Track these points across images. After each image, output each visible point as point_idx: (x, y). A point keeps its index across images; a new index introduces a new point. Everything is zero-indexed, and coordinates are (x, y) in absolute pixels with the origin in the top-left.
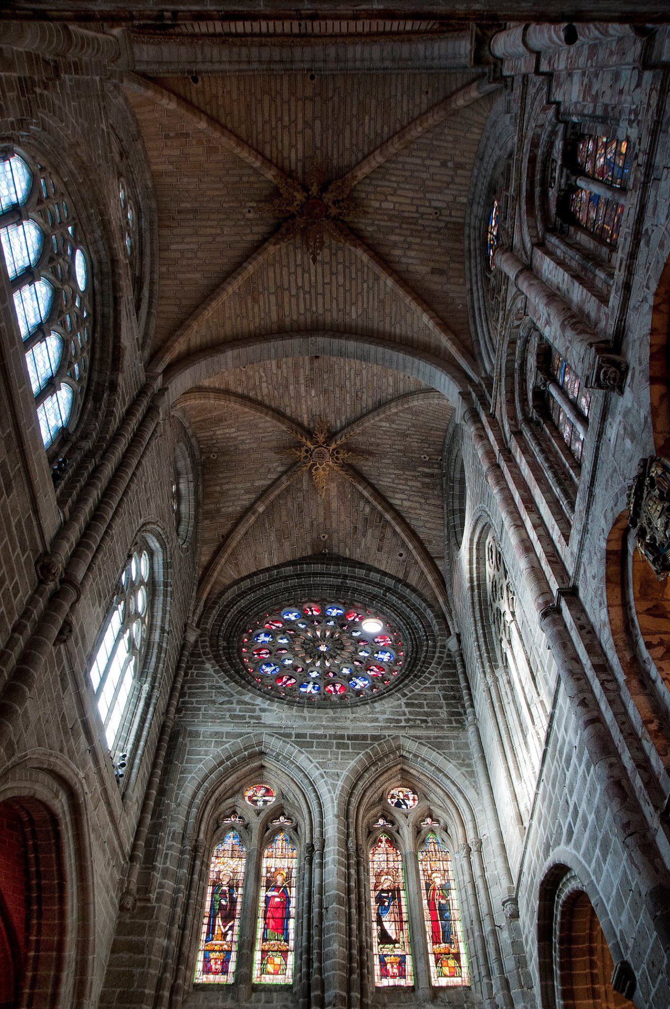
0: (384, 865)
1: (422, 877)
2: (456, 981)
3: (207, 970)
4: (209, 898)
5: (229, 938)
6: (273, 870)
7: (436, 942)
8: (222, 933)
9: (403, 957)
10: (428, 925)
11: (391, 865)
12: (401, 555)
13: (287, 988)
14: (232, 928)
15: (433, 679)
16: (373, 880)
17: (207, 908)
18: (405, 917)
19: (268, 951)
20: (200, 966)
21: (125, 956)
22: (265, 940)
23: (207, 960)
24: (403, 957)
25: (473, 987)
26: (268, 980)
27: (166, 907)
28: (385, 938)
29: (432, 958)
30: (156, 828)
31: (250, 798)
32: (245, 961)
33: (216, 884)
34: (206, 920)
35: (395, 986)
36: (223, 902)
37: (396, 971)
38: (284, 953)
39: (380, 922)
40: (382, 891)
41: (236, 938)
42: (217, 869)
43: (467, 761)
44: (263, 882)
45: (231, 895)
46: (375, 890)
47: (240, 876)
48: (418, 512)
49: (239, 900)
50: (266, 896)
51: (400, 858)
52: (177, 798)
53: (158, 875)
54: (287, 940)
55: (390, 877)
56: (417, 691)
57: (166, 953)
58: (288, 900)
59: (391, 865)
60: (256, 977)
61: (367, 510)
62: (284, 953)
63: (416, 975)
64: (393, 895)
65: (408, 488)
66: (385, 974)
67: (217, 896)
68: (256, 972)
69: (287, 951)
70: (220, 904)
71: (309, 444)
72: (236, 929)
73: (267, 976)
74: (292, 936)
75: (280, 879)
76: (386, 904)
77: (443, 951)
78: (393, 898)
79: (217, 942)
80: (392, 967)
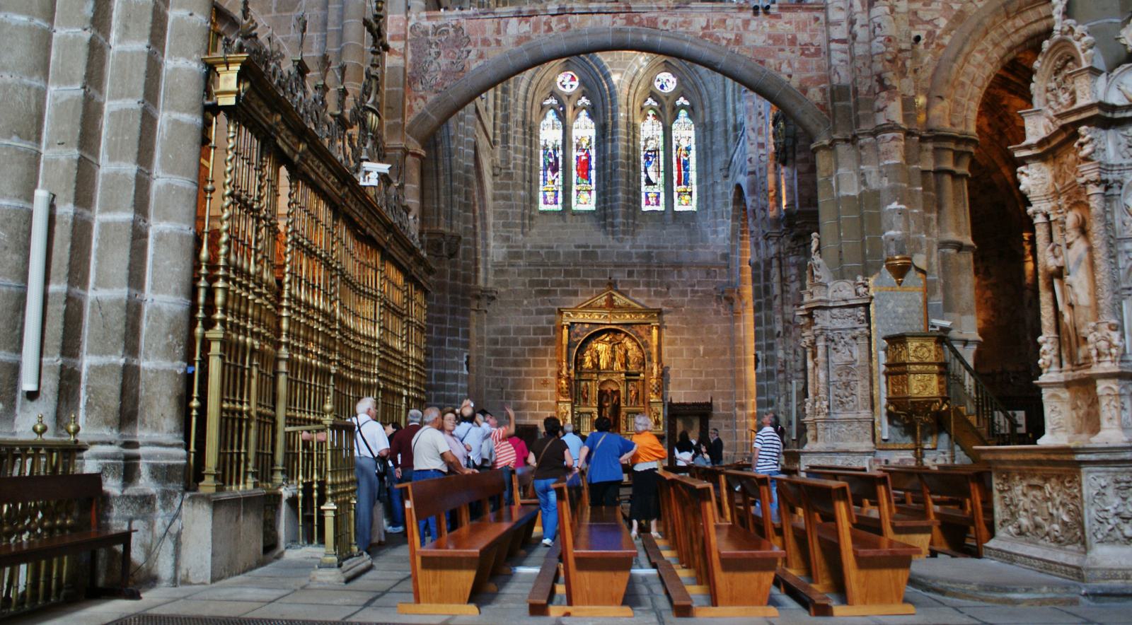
16: (643, 144)
21: (501, 202)
23: (545, 197)
27: (520, 172)
28: (649, 182)
30: (506, 118)
32: (567, 198)
33: (546, 148)
34: (541, 172)
38: (589, 192)
39: (646, 171)
41: (561, 183)
47: (560, 143)
53: (511, 152)
57: (524, 199)
60: (575, 206)
62: (589, 192)
63: (666, 204)
66: (648, 203)
72: (561, 177)
79: (550, 185)
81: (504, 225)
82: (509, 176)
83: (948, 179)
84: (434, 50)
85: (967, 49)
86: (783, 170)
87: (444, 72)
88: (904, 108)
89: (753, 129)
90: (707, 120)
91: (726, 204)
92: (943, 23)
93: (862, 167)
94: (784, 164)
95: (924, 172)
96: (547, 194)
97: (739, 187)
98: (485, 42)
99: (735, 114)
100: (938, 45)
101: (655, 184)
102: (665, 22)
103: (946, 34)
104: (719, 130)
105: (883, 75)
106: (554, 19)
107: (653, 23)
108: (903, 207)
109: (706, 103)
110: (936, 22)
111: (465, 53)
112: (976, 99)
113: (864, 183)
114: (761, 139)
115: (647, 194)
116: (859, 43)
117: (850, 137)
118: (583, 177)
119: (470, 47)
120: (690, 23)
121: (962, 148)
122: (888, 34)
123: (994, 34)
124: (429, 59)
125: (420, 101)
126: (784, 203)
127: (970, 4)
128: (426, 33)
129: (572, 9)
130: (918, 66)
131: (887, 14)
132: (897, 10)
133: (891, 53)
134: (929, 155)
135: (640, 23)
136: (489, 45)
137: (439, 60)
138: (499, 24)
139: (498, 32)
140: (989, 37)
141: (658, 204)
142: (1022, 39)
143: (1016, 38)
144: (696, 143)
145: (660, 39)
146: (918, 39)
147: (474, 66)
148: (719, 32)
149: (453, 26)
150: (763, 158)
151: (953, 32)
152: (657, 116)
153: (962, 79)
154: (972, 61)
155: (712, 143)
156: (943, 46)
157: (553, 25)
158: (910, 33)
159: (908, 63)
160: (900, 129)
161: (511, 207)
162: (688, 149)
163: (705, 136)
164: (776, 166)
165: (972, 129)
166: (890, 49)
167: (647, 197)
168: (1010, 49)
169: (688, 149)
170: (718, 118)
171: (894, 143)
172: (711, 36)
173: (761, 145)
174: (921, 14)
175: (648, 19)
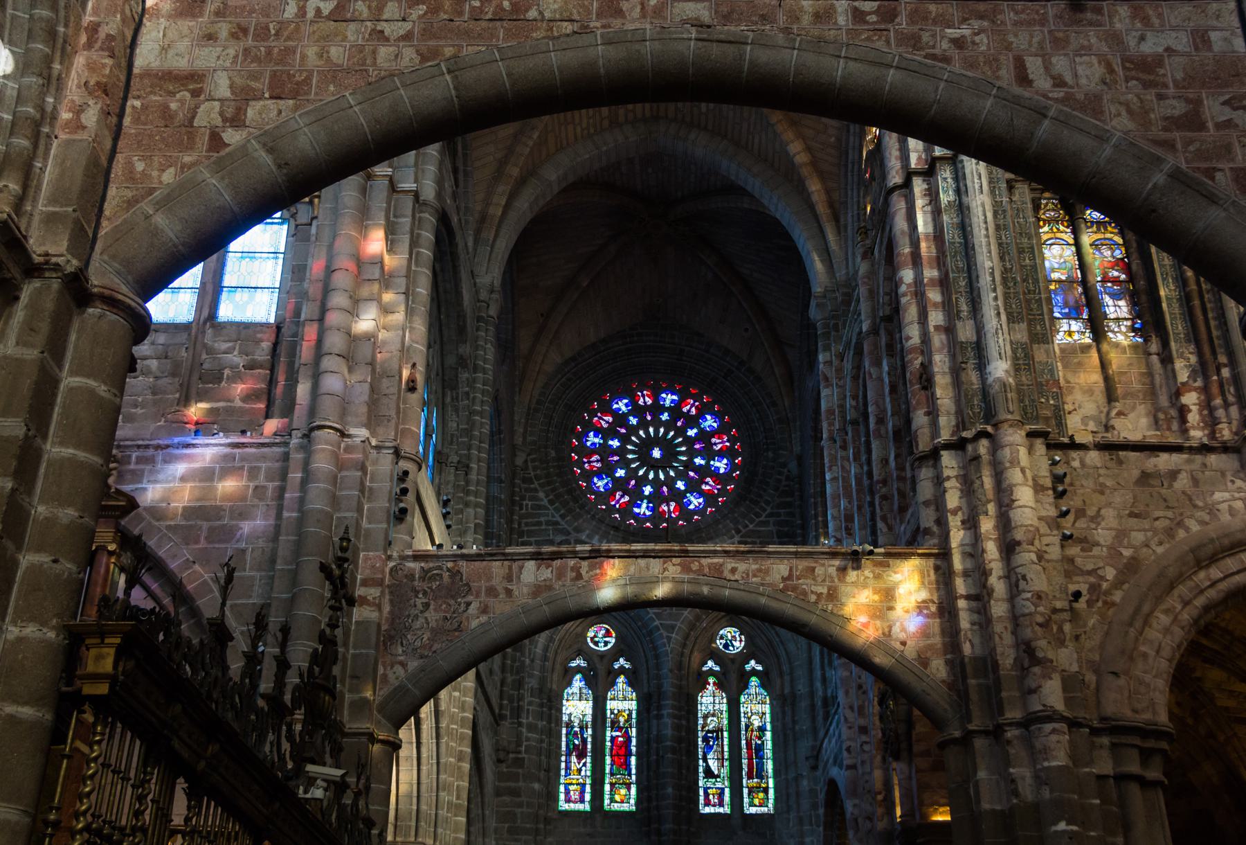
0: (711, 707)
1: (743, 719)
2: (764, 810)
3: (568, 800)
4: (564, 739)
6: (616, 712)
7: (750, 777)
10: (745, 762)
11: (717, 707)
13: (629, 813)
14: (585, 765)
15: (769, 510)
16: (701, 721)
17: (564, 748)
19: (616, 783)
20: (562, 797)
21: (507, 799)
22: (612, 774)
23: (567, 792)
24: (723, 790)
26: (616, 807)
28: (709, 773)
31: (592, 639)
33: (569, 725)
34: (563, 758)
36: (576, 742)
38: (628, 787)
39: (705, 760)
40: (709, 731)
41: (589, 773)
42: (568, 712)
44: (608, 724)
45: (582, 735)
46: (702, 731)
47: (589, 718)
49: (589, 739)
51: (725, 700)
52: (530, 654)
54: (630, 775)
55: (715, 719)
56: (751, 526)
58: (629, 739)
59: (717, 707)
62: (628, 787)
66: (707, 803)
68: (607, 802)
69: (631, 783)
70: (574, 744)
72: (589, 765)
73: (616, 805)
74: (634, 771)
79: (574, 777)
81: (510, 831)
82: (519, 762)
83: (1134, 789)
84: (420, 601)
85: (1146, 608)
86: (895, 765)
87: (433, 630)
88: (1065, 689)
89: (851, 708)
90: (787, 691)
91: (815, 806)
92: (1110, 573)
93: (1011, 770)
94: (897, 758)
95: (1100, 778)
96: (571, 788)
97: (832, 784)
98: (492, 592)
99: (824, 680)
100: (1105, 603)
101: (718, 776)
102: (733, 570)
103: (1116, 589)
104: (804, 704)
105: (1033, 644)
106: (585, 564)
107: (717, 570)
108: (1075, 828)
109: (785, 668)
110: (1100, 572)
111: (463, 606)
112: (1165, 676)
113: (1016, 793)
114: (862, 722)
115: (706, 790)
116: (997, 600)
117: (991, 728)
118: (620, 766)
119: (470, 598)
120: (767, 572)
121: (1151, 744)
122: (1036, 588)
123: (1182, 589)
124: (414, 612)
125: (399, 670)
126: (898, 812)
127: (1145, 550)
128: (411, 577)
129: (609, 551)
130: (1080, 631)
131: (1033, 563)
132: (1047, 556)
133: (1042, 614)
134: (1105, 754)
135: (700, 571)
136: (496, 596)
137: (426, 615)
138: (510, 568)
139: (509, 578)
140: (1176, 592)
141: (721, 804)
142: (1222, 595)
143: (1212, 594)
144: (772, 722)
145: (727, 592)
146: (1077, 595)
147: (474, 624)
148: (805, 584)
149: (448, 570)
150: (866, 748)
151: (1126, 586)
152: (720, 685)
153: (1143, 648)
154: (1155, 624)
155: (794, 722)
156: (1113, 604)
157: (583, 572)
158: (1067, 588)
159: (1067, 627)
160: (1063, 719)
161: (520, 805)
162: (762, 729)
163: (784, 713)
164: (884, 759)
165: (1163, 718)
166: (1041, 609)
167: (706, 795)
168: (1207, 609)
169: (762, 729)
171: (1054, 738)
172: (794, 589)
173: (864, 730)
174: (1079, 561)
175: (710, 566)
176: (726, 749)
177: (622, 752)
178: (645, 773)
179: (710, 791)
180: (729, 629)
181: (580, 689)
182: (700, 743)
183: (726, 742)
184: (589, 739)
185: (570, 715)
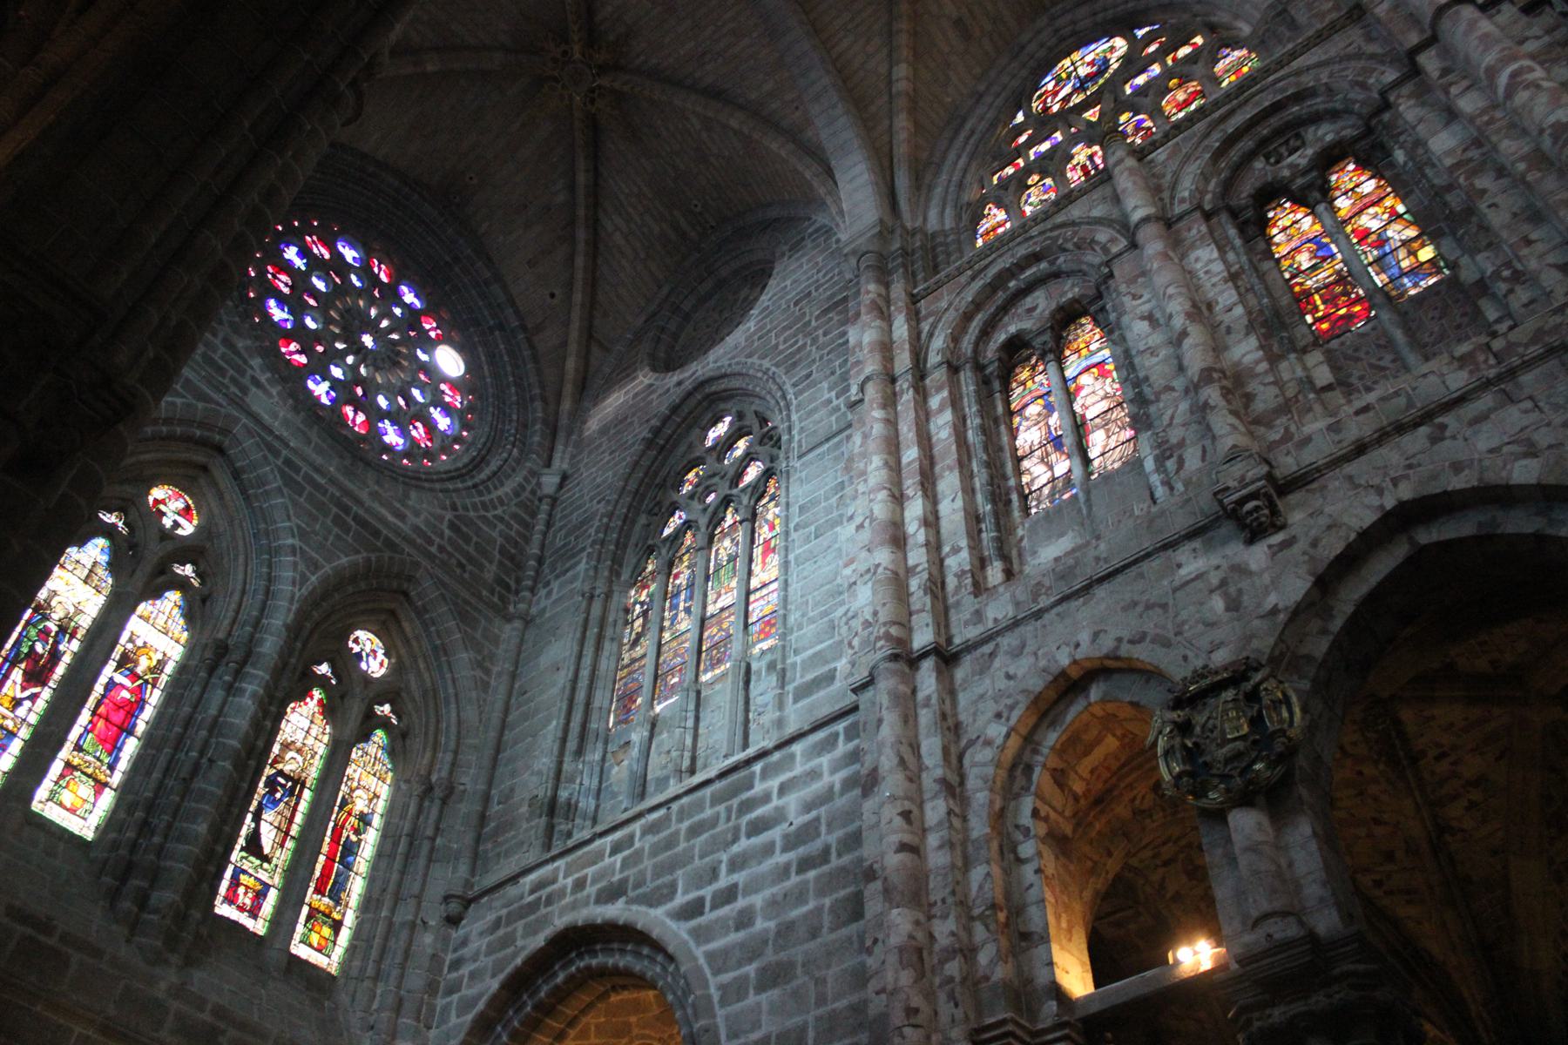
0: (300, 736)
5: (21, 711)
8: (14, 698)
9: (267, 887)
10: (322, 859)
12: (552, 296)
15: (499, 512)
18: (294, 831)
19: (76, 768)
22: (78, 748)
24: (267, 887)
25: (342, 981)
26: (53, 813)
28: (254, 846)
29: (305, 910)
33: (43, 611)
35: (235, 923)
36: (39, 648)
37: (248, 902)
38: (100, 786)
39: (257, 818)
40: (281, 773)
41: (33, 719)
43: (487, 664)
44: (116, 655)
45: (56, 643)
47: (85, 622)
48: (624, 262)
50: (111, 679)
51: (326, 739)
54: (112, 767)
55: (300, 759)
56: (472, 514)
58: (140, 703)
59: (310, 741)
61: (561, 198)
62: (100, 786)
64: (293, 789)
65: (639, 222)
66: (231, 899)
67: (33, 632)
68: (42, 793)
69: (106, 785)
70: (32, 648)
71: (576, 48)
72: (41, 705)
74: (123, 765)
75: (143, 664)
76: (278, 795)
77: (322, 908)
78: (291, 792)
80: (246, 894)
101: (267, 859)
104: (466, 808)
115: (238, 871)
118: (102, 740)
152: (328, 710)
162: (365, 819)
167: (235, 882)
170: (469, 780)
176: (299, 818)
177: (118, 717)
178: (156, 775)
179: (243, 878)
180: (371, 636)
181: (95, 563)
182: (261, 785)
183: (303, 806)
184: (67, 659)
185: (55, 593)
